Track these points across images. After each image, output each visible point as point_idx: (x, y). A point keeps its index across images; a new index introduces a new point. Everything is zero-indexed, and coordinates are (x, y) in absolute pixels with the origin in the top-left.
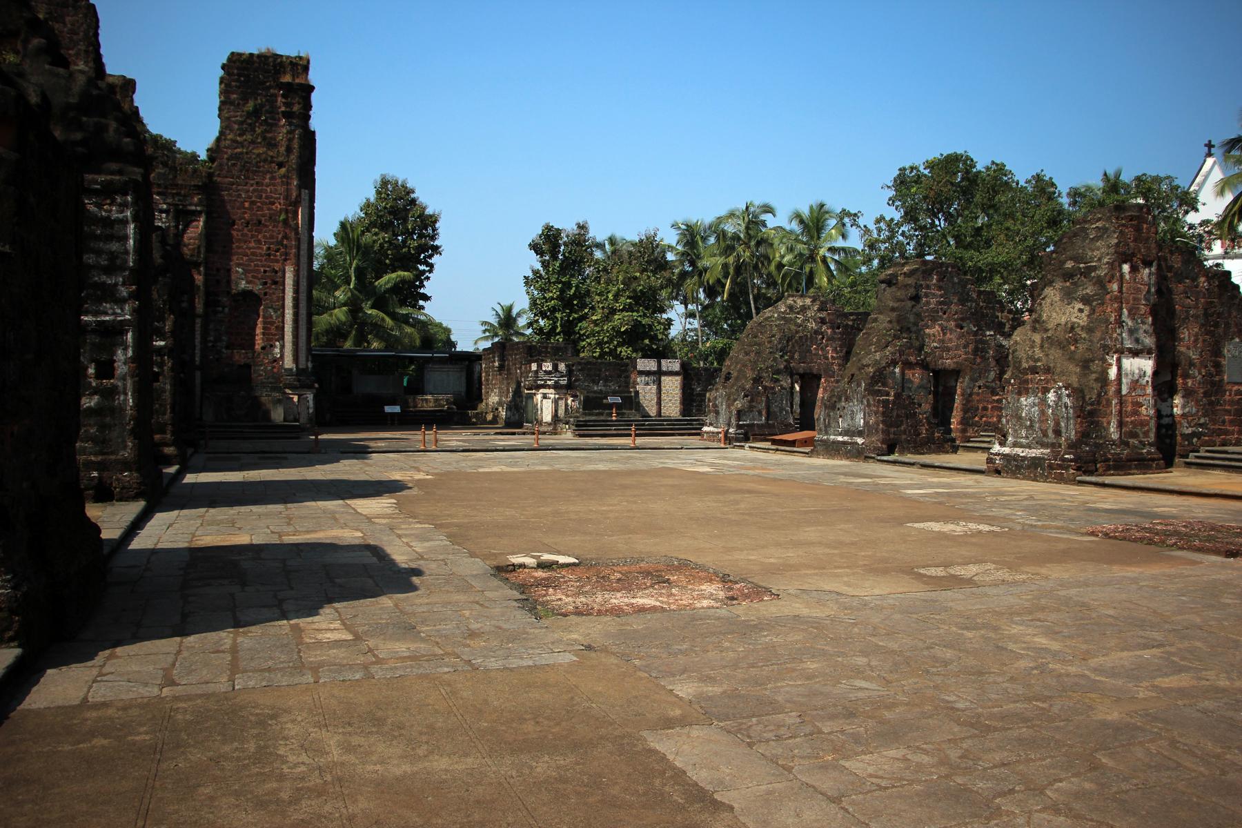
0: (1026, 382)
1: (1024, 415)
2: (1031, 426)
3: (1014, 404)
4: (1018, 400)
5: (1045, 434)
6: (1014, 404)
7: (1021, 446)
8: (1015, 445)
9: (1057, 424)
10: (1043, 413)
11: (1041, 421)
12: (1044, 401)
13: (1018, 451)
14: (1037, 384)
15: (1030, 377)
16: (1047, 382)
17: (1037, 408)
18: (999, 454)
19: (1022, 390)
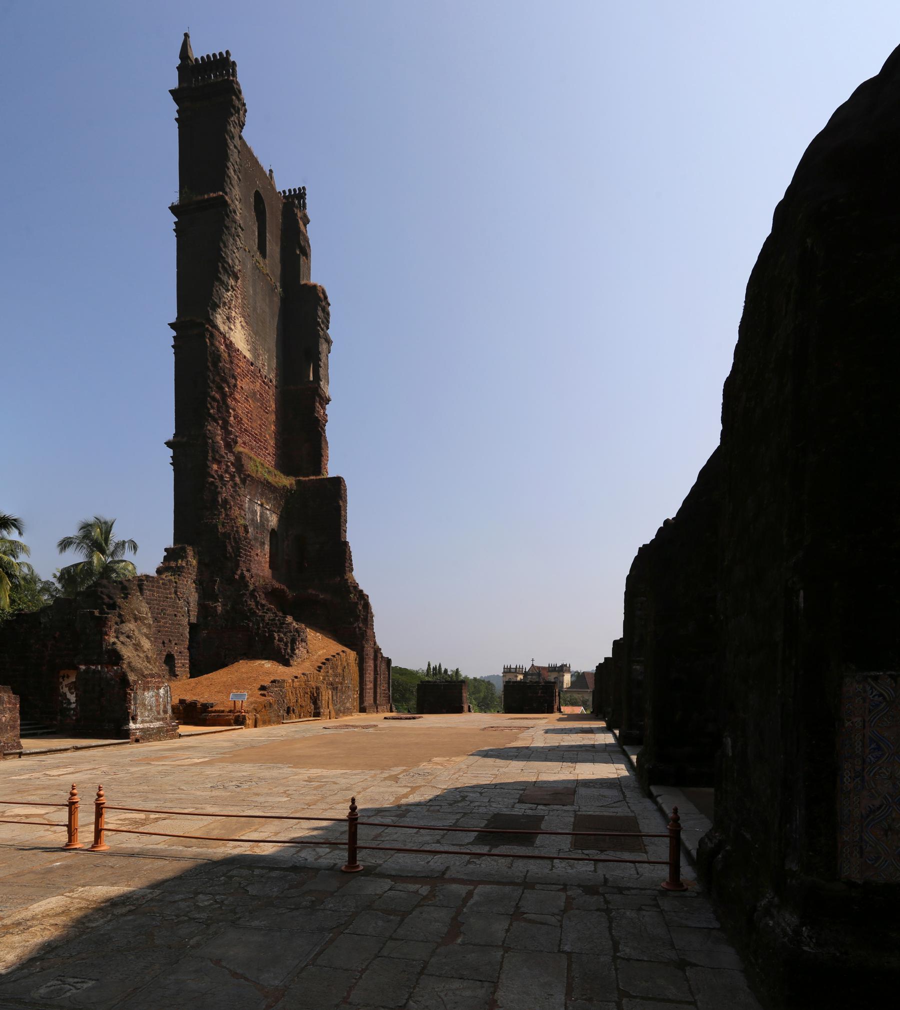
0: (148, 682)
1: (146, 703)
2: (151, 709)
3: (141, 696)
4: (143, 694)
5: (159, 713)
6: (141, 696)
7: (147, 722)
8: (143, 722)
9: (165, 706)
10: (157, 700)
11: (157, 706)
12: (158, 695)
13: (146, 725)
14: (154, 684)
15: (149, 679)
16: (159, 682)
17: (154, 698)
18: (138, 729)
19: (146, 688)
